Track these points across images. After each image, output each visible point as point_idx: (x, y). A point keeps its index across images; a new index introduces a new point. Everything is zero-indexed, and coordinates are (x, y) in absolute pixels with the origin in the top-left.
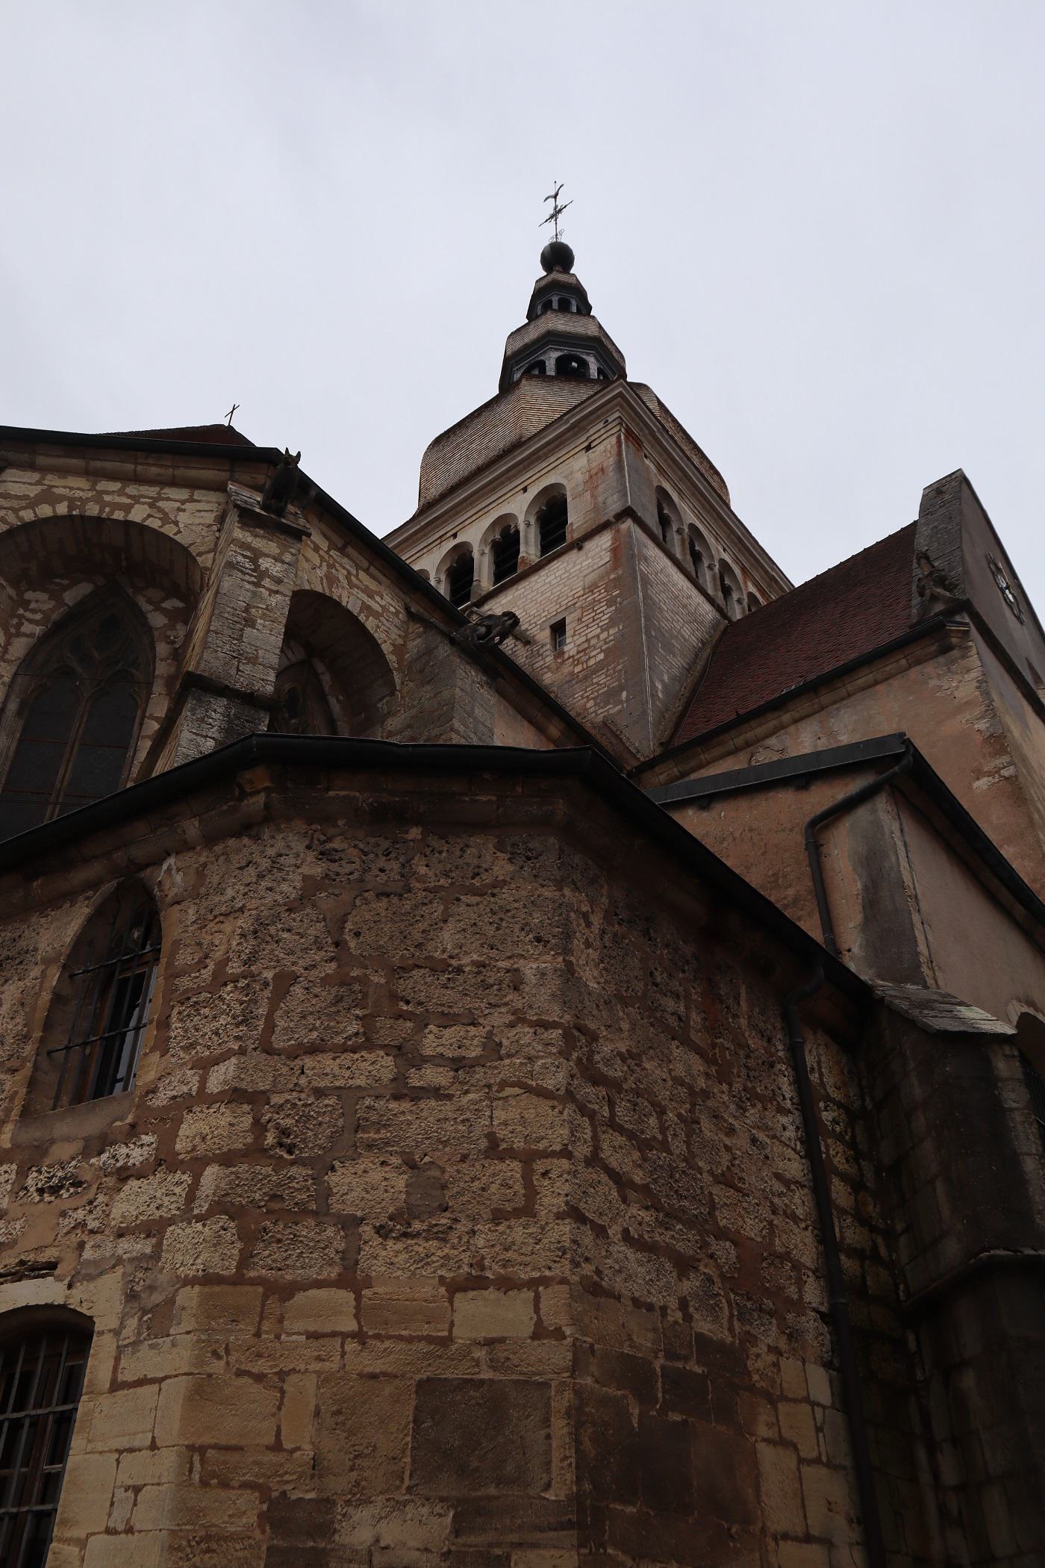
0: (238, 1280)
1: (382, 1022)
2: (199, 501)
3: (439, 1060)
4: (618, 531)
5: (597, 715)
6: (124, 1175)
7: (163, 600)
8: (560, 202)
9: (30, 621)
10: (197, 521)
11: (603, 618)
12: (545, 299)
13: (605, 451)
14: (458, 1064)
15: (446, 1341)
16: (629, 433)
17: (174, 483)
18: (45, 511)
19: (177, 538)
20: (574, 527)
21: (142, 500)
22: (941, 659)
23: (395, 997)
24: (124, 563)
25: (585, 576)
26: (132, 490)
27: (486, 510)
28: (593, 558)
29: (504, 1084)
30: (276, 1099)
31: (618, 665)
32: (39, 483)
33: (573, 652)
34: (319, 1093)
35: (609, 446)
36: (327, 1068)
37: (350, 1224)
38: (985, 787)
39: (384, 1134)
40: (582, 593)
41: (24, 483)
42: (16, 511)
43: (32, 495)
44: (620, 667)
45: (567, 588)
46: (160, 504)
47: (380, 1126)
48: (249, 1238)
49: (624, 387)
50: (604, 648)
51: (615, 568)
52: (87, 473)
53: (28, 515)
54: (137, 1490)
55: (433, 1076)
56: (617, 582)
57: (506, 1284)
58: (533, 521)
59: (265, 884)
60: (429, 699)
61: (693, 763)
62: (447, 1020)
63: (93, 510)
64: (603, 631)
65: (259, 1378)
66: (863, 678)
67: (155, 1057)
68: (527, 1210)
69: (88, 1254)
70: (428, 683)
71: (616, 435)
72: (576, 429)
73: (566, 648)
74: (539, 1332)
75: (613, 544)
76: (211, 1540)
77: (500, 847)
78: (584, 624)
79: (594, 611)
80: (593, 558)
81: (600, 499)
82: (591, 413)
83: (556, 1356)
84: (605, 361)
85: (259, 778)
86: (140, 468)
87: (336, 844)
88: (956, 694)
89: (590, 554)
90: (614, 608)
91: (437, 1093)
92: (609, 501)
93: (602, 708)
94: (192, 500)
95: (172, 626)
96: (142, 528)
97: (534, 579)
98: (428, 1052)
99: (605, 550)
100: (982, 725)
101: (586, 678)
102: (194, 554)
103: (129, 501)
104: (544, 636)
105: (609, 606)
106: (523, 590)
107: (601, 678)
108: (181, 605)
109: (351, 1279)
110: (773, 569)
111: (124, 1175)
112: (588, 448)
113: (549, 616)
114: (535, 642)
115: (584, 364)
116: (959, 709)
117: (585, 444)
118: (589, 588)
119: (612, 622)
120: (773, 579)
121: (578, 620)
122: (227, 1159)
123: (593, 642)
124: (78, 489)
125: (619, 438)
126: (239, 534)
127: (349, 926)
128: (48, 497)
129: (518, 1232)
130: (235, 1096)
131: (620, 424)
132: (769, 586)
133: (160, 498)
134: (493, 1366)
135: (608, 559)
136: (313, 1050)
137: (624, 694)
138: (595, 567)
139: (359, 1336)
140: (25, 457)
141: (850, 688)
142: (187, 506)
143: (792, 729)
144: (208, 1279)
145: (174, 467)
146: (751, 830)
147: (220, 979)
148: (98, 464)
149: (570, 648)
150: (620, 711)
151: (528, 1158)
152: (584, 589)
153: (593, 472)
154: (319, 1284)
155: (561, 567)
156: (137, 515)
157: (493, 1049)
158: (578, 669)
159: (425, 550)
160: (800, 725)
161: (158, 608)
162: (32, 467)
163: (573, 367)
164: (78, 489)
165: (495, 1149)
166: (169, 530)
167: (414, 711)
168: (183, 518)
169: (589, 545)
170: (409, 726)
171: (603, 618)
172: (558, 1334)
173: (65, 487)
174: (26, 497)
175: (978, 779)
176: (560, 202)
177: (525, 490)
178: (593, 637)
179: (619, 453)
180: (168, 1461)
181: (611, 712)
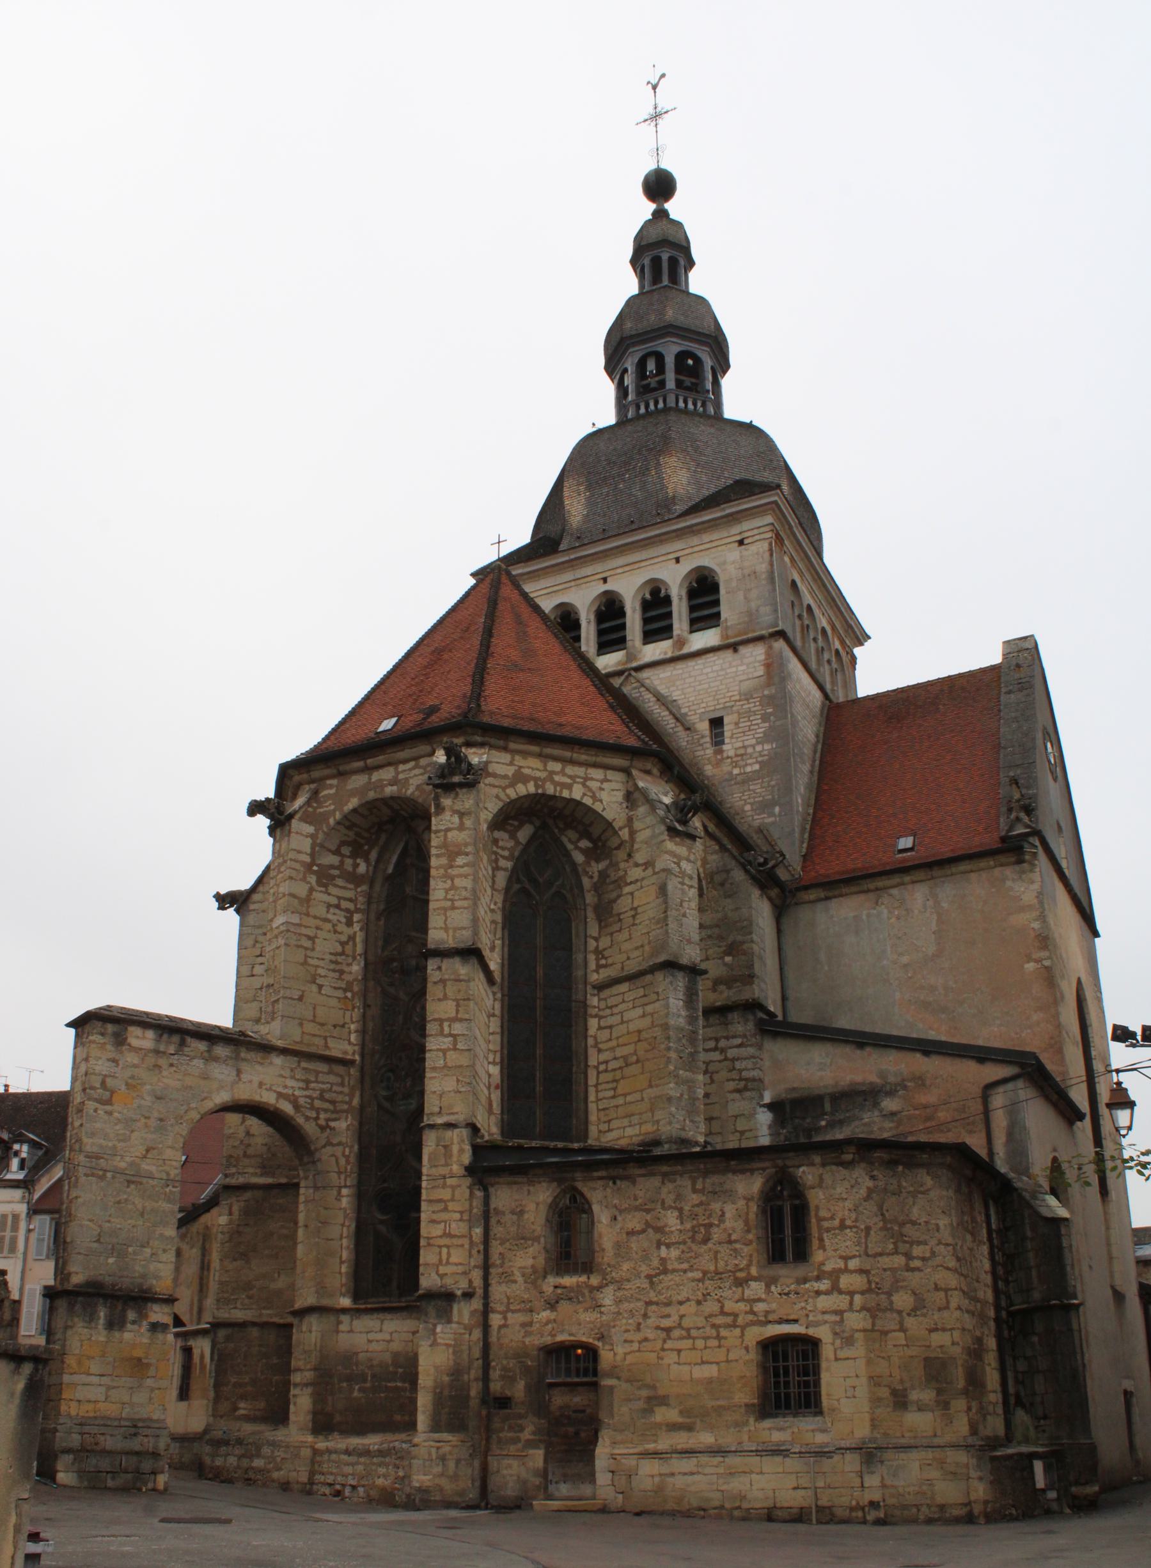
0: (873, 1330)
1: (900, 1245)
2: (610, 781)
3: (918, 1258)
4: (770, 647)
5: (753, 820)
6: (818, 1293)
7: (579, 840)
9: (504, 857)
10: (614, 799)
11: (758, 731)
13: (757, 554)
14: (924, 1259)
15: (929, 1347)
16: (778, 535)
17: (595, 765)
18: (522, 790)
19: (604, 814)
20: (729, 624)
21: (578, 780)
22: (1017, 868)
23: (902, 1235)
24: (555, 814)
25: (741, 681)
26: (571, 770)
27: (637, 566)
28: (748, 665)
29: (938, 1266)
30: (873, 1272)
31: (771, 780)
32: (511, 764)
33: (731, 753)
34: (885, 1270)
35: (761, 550)
36: (885, 1261)
37: (900, 1312)
38: (1032, 969)
39: (905, 1284)
40: (737, 698)
42: (504, 789)
43: (510, 774)
44: (773, 783)
45: (724, 687)
46: (589, 783)
47: (904, 1280)
48: (874, 1317)
50: (760, 759)
51: (769, 684)
52: (539, 755)
53: (512, 793)
54: (854, 1387)
55: (916, 1263)
56: (770, 700)
57: (944, 1330)
58: (684, 593)
59: (855, 1190)
60: (732, 910)
61: (836, 892)
62: (919, 1243)
63: (550, 789)
64: (758, 743)
65: (883, 1358)
66: (963, 866)
67: (821, 1251)
68: (947, 1308)
69: (811, 1318)
70: (730, 896)
71: (768, 541)
72: (731, 518)
73: (725, 747)
74: (953, 1344)
75: (766, 659)
76: (879, 1399)
77: (928, 1173)
78: (740, 730)
79: (749, 721)
80: (748, 665)
81: (753, 605)
82: (746, 510)
83: (957, 1351)
84: (718, 360)
85: (852, 1149)
86: (575, 755)
87: (875, 1173)
88: (1022, 897)
89: (746, 661)
90: (767, 725)
91: (918, 1269)
92: (763, 610)
93: (759, 815)
94: (606, 780)
95: (588, 863)
96: (578, 803)
97: (691, 663)
98: (915, 1255)
99: (759, 662)
100: (1036, 925)
101: (744, 782)
102: (617, 829)
103: (569, 781)
104: (704, 727)
105: (764, 721)
106: (680, 671)
107: (756, 787)
108: (590, 845)
109: (902, 1329)
110: (851, 618)
111: (818, 1293)
112: (741, 543)
113: (707, 709)
114: (696, 731)
115: (698, 361)
116: (1023, 909)
117: (738, 538)
118: (745, 695)
119: (766, 738)
120: (850, 627)
121: (737, 724)
122: (862, 1293)
123: (750, 750)
124: (538, 769)
125: (770, 544)
126: (670, 845)
127: (885, 1208)
128: (520, 777)
129: (946, 1314)
130: (861, 1271)
131: (772, 531)
132: (846, 631)
133: (586, 779)
134: (942, 1353)
135: (761, 673)
136: (881, 1254)
137: (777, 809)
138: (750, 676)
139: (907, 1346)
140: (501, 743)
141: (954, 870)
142: (605, 785)
143: (910, 887)
144: (865, 1331)
145: (596, 755)
146: (952, 1077)
147: (842, 1226)
148: (548, 751)
149: (728, 748)
150: (773, 823)
151: (946, 1290)
152: (740, 694)
153: (746, 572)
154: (894, 1331)
155: (717, 662)
156: (577, 793)
157: (933, 1253)
158: (736, 771)
159: (573, 583)
160: (917, 886)
161: (577, 848)
162: (505, 749)
163: (688, 365)
164: (538, 769)
165: (937, 1288)
166: (598, 807)
167: (719, 915)
168: (604, 796)
169: (744, 650)
170: (717, 926)
171: (758, 731)
172: (958, 1344)
173: (529, 767)
174: (505, 777)
175: (1028, 962)
177: (677, 560)
178: (751, 746)
179: (771, 565)
180: (864, 1380)
181: (766, 821)
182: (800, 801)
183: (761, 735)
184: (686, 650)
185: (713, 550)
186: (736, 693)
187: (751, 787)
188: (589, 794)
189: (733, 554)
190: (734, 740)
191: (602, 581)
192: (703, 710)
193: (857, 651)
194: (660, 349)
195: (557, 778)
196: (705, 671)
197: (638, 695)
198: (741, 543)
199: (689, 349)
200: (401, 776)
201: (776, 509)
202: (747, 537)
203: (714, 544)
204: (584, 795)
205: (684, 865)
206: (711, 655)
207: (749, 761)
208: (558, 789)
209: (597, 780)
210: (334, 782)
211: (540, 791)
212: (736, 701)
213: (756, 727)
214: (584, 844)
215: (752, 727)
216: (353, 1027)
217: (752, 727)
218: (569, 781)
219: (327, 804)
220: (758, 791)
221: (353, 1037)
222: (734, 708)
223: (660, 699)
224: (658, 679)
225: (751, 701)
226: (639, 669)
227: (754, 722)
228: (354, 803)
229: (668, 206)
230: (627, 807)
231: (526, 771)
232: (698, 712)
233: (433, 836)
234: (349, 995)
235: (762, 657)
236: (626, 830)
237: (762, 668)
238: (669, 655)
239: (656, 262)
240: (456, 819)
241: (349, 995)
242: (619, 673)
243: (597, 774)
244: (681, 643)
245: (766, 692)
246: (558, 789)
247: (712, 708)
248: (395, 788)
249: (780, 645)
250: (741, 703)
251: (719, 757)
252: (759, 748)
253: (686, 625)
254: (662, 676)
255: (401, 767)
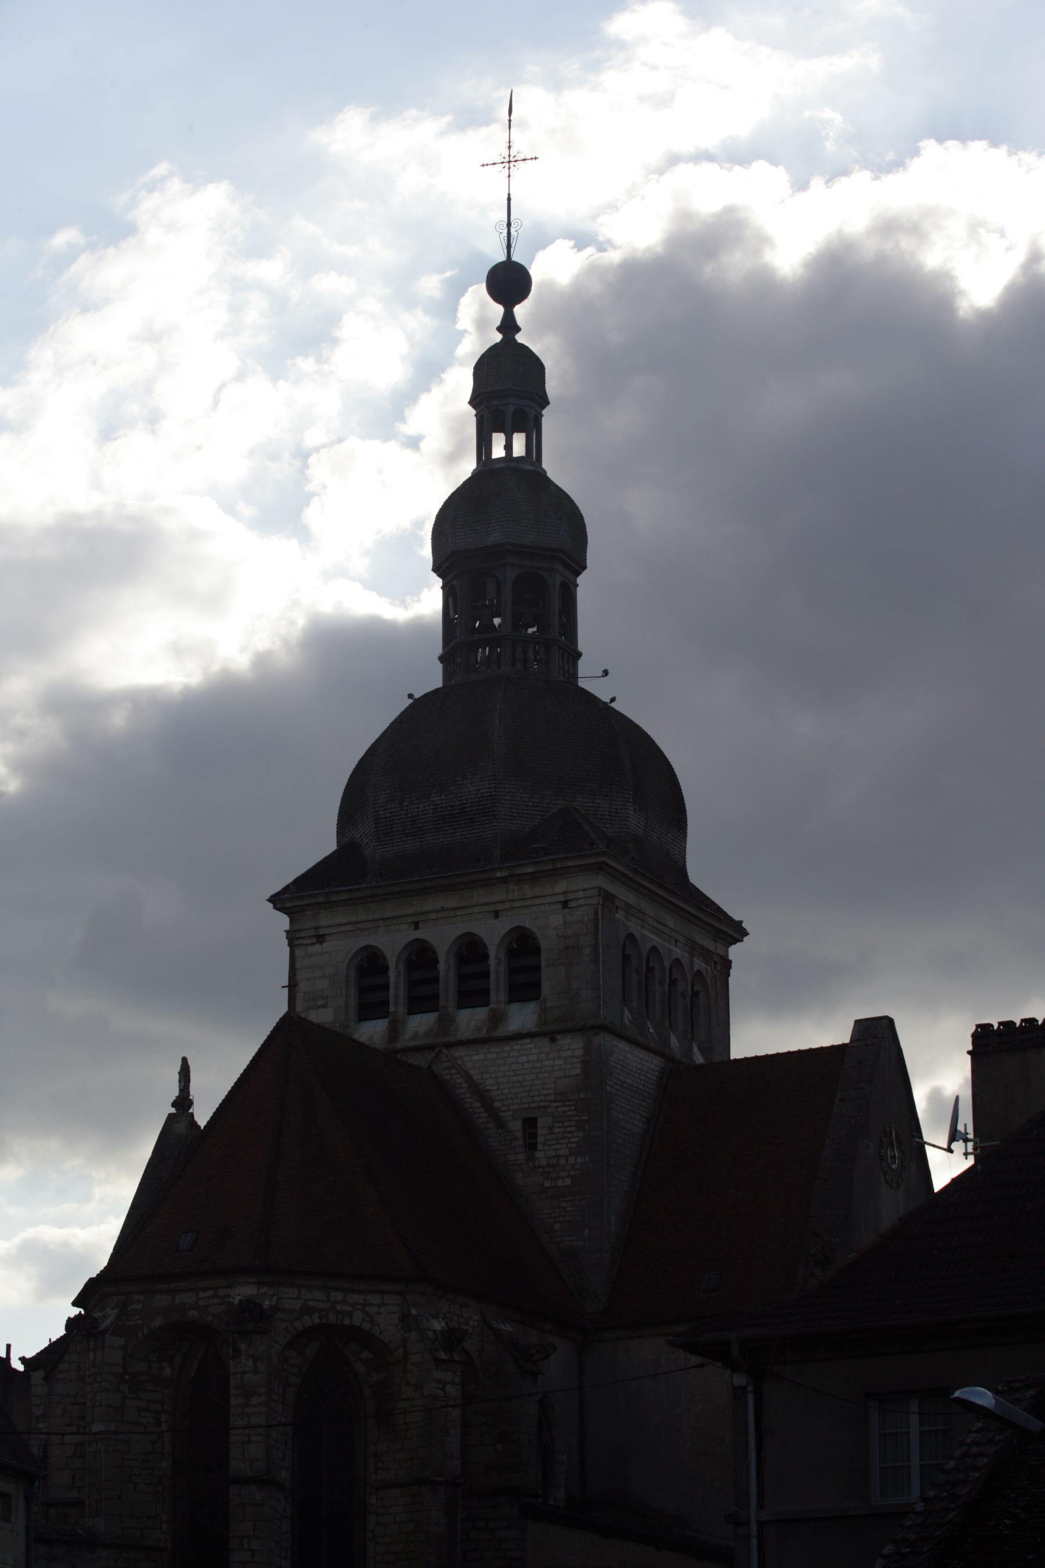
2: (387, 1305)
21: (358, 1307)
25: (557, 1078)
33: (544, 1162)
40: (552, 1097)
41: (291, 1299)
43: (297, 1309)
46: (367, 1309)
50: (572, 1173)
63: (332, 1318)
90: (581, 1134)
94: (383, 1304)
103: (350, 1309)
104: (516, 1126)
106: (495, 1056)
112: (565, 904)
117: (562, 898)
121: (550, 1128)
123: (562, 1161)
125: (596, 912)
137: (586, 1232)
149: (541, 1156)
155: (534, 1051)
156: (357, 1319)
158: (547, 1184)
169: (564, 1041)
182: (613, 1219)
183: (574, 1145)
184: (500, 1032)
185: (535, 909)
186: (551, 1091)
187: (563, 1204)
188: (369, 1319)
189: (556, 919)
190: (546, 1148)
191: (413, 927)
192: (516, 1107)
193: (735, 952)
195: (338, 1307)
196: (521, 1059)
197: (449, 1077)
198: (565, 904)
200: (201, 1303)
202: (572, 900)
203: (537, 902)
204: (363, 1320)
205: (449, 1388)
206: (528, 1040)
207: (562, 1174)
208: (340, 1317)
209: (376, 1306)
210: (141, 1298)
211: (323, 1321)
212: (550, 1101)
213: (570, 1135)
214: (365, 1355)
215: (566, 1135)
216: (164, 1517)
217: (566, 1135)
218: (350, 1309)
219: (135, 1318)
220: (568, 1209)
221: (164, 1526)
222: (549, 1110)
223: (474, 1086)
224: (473, 1059)
225: (566, 1103)
226: (449, 1046)
227: (568, 1129)
228: (158, 1322)
229: (520, 311)
230: (402, 1328)
231: (311, 1304)
232: (512, 1108)
233: (232, 1378)
234: (160, 1489)
235: (580, 1052)
236: (401, 1350)
237: (579, 1065)
238: (484, 1033)
240: (250, 1363)
241: (160, 1489)
242: (430, 1048)
243: (375, 1299)
244: (496, 1019)
245: (582, 1096)
246: (340, 1317)
247: (526, 1106)
248: (196, 1313)
250: (556, 1104)
251: (531, 1165)
252: (571, 1160)
253: (503, 996)
254: (475, 1058)
255: (201, 1294)
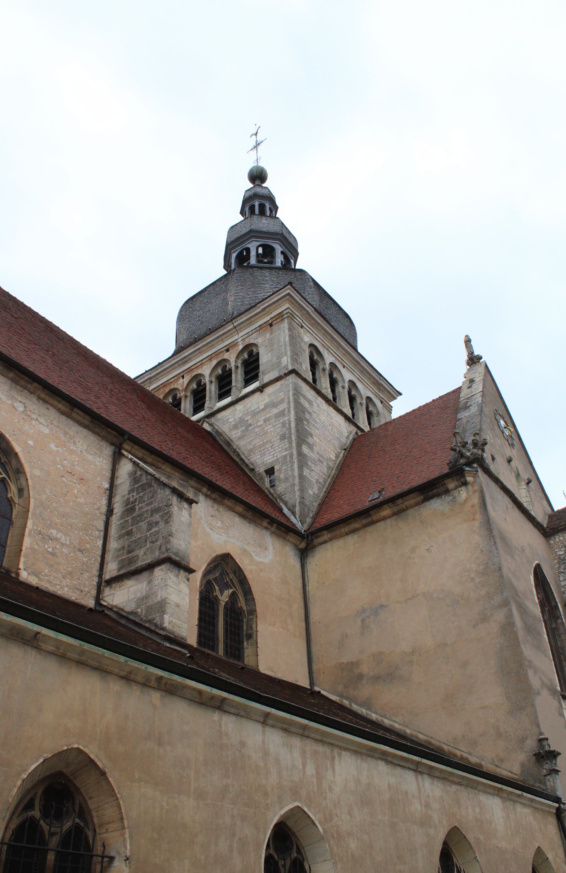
8: (260, 138)
12: (251, 203)
49: (291, 290)
115: (272, 249)
176: (260, 138)
194: (248, 246)
199: (266, 243)
201: (290, 299)
239: (252, 208)
249: (292, 378)
